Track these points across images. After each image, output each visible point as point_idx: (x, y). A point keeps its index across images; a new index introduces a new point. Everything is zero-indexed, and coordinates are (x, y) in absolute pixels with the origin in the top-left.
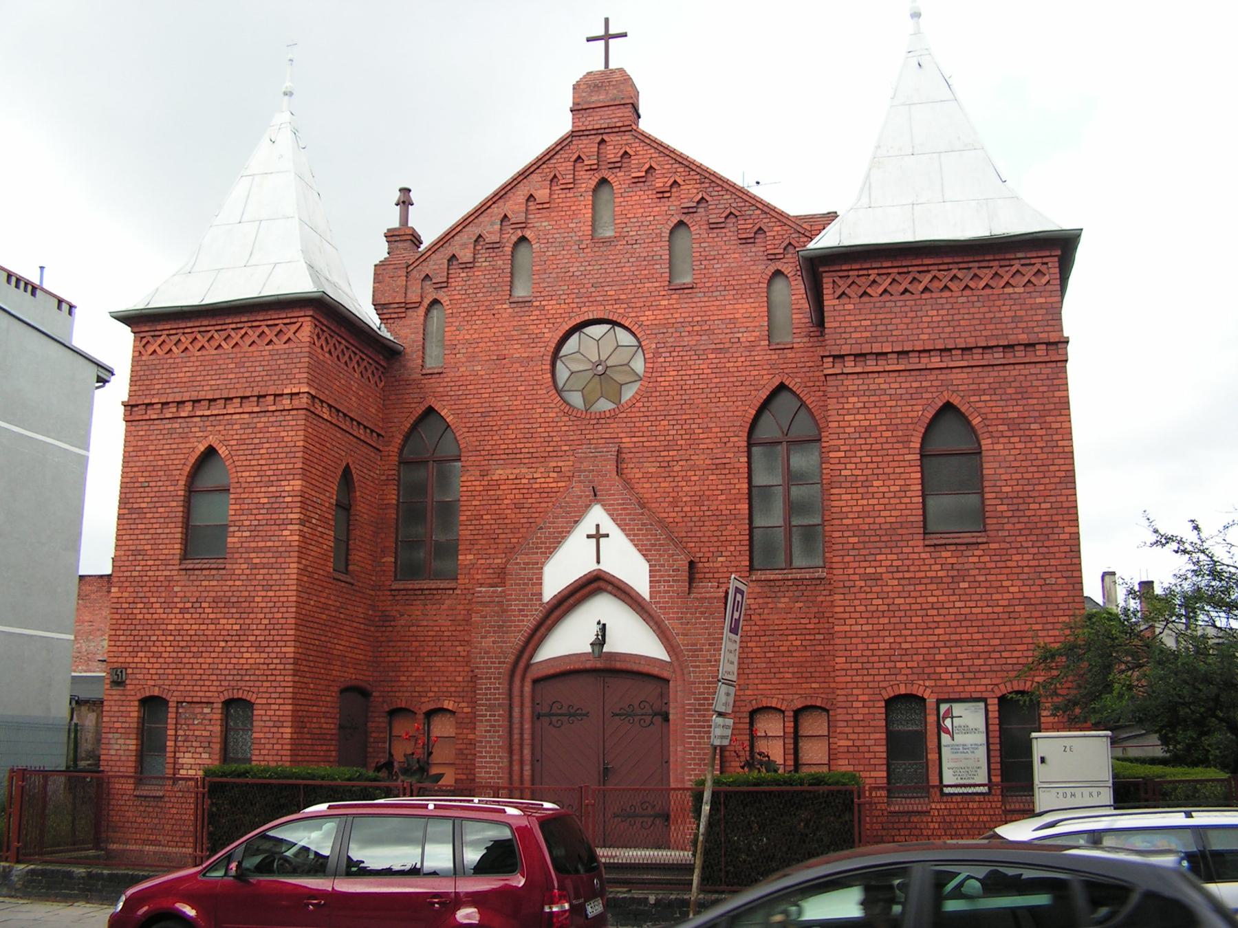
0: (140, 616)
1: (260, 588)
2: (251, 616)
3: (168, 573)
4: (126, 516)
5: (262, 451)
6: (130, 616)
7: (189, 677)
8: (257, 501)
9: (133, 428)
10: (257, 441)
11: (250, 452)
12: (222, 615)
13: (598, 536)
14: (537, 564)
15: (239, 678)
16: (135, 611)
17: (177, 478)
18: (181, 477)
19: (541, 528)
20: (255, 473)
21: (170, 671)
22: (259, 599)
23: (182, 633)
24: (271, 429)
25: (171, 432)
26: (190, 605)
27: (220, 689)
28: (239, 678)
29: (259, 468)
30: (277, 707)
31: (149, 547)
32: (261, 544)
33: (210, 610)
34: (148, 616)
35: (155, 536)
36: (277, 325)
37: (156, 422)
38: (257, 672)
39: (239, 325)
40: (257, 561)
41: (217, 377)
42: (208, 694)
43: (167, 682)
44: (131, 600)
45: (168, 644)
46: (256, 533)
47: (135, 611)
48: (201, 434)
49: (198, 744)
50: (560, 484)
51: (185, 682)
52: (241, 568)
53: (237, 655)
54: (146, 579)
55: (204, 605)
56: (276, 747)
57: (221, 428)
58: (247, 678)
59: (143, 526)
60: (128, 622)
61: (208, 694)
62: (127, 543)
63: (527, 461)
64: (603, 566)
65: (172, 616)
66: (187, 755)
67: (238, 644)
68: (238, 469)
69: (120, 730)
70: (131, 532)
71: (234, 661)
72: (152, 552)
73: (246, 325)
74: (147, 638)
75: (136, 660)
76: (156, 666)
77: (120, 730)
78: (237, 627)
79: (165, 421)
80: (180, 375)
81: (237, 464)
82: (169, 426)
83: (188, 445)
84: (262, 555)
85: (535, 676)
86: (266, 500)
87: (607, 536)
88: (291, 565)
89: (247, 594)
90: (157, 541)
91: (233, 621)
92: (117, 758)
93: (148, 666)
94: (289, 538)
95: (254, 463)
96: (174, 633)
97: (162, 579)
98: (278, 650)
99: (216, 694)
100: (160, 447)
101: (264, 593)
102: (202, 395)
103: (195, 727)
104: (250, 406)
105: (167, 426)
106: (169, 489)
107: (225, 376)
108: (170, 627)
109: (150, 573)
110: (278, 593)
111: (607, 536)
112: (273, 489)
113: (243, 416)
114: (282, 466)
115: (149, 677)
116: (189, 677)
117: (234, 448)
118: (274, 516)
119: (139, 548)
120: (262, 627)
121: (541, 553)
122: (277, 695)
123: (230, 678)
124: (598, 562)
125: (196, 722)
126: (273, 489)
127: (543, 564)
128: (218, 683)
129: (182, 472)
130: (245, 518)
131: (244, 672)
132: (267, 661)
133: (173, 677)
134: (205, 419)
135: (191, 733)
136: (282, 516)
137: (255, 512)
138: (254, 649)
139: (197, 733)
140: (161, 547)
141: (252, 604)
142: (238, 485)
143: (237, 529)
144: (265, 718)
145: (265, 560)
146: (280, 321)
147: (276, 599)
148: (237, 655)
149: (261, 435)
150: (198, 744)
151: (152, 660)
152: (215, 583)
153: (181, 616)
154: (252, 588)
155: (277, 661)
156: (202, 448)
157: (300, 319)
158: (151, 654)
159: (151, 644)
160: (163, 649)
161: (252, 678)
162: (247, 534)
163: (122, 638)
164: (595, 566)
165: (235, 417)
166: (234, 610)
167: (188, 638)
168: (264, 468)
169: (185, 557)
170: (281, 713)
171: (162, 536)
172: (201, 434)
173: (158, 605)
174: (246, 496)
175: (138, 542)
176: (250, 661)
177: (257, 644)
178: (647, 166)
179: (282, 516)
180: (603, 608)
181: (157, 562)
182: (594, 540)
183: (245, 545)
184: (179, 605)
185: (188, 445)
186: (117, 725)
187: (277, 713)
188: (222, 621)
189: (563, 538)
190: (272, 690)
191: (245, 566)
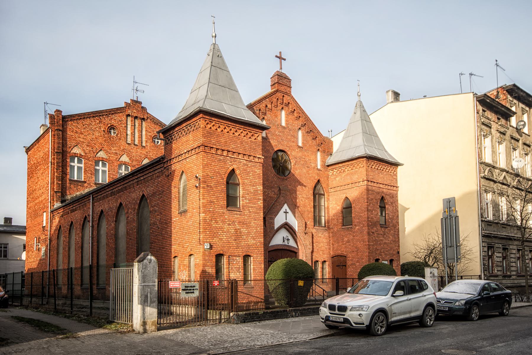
0: (214, 225)
1: (253, 219)
2: (250, 228)
3: (223, 211)
4: (206, 188)
5: (251, 174)
6: (210, 225)
7: (232, 247)
8: (250, 191)
9: (205, 155)
10: (248, 170)
11: (246, 174)
12: (242, 227)
13: (286, 212)
14: (273, 218)
15: (248, 248)
16: (212, 223)
17: (223, 177)
18: (225, 177)
19: (274, 208)
20: (249, 181)
21: (226, 245)
22: (253, 223)
23: (229, 232)
24: (252, 168)
25: (220, 160)
26: (231, 223)
27: (242, 252)
28: (248, 248)
29: (250, 180)
30: (259, 258)
31: (215, 201)
32: (252, 205)
33: (238, 225)
34: (217, 225)
35: (217, 197)
36: (252, 132)
37: (214, 155)
38: (253, 247)
39: (240, 128)
40: (251, 210)
41: (234, 144)
42: (239, 253)
43: (225, 249)
44: (210, 219)
45: (224, 236)
46: (250, 201)
47: (212, 223)
48: (230, 163)
49: (236, 270)
50: (275, 196)
51: (231, 249)
52: (247, 212)
53: (247, 241)
54: (214, 212)
55: (236, 223)
56: (260, 270)
57: (237, 163)
58: (251, 248)
59: (212, 193)
60: (210, 227)
61: (239, 253)
62: (207, 198)
63: (267, 187)
64: (287, 221)
65: (225, 226)
66: (232, 274)
67: (247, 237)
68: (244, 179)
69: (209, 266)
70: (208, 194)
71: (246, 243)
72: (217, 203)
73: (242, 129)
74: (217, 233)
75: (213, 241)
76: (221, 243)
77: (209, 266)
78: (247, 232)
79: (217, 155)
80: (221, 140)
81: (244, 177)
82: (219, 158)
83: (226, 166)
84: (252, 209)
85: (269, 250)
86: (253, 191)
87: (288, 213)
88: (261, 213)
89: (249, 221)
90: (218, 199)
91: (245, 229)
92: (209, 276)
93: (218, 243)
94: (260, 205)
95: (248, 178)
96: (226, 232)
97: (221, 212)
98: (259, 240)
99: (241, 253)
100: (216, 165)
101: (254, 221)
102: (230, 149)
103: (235, 264)
104: (246, 158)
105: (218, 157)
106: (221, 181)
107: (237, 145)
108: (225, 230)
109: (216, 210)
110: (258, 222)
111: (288, 213)
112: (255, 188)
113: (243, 161)
114: (257, 181)
115: (219, 247)
116: (232, 247)
117: (242, 171)
118: (256, 197)
119: (212, 200)
120: (254, 232)
121: (274, 215)
122: (259, 254)
123: (245, 248)
124: (286, 220)
125: (234, 263)
126: (255, 188)
127: (275, 218)
128: (242, 250)
129: (225, 176)
130: (247, 196)
131: (249, 246)
132: (256, 243)
133: (227, 247)
134: (232, 158)
135: (233, 266)
136: (258, 197)
137: (250, 194)
138: (252, 239)
139: (235, 266)
140: (220, 201)
141: (251, 225)
142: (244, 184)
143: (244, 199)
144: (256, 261)
145: (253, 211)
146: (253, 131)
147: (258, 224)
148: (247, 241)
149: (250, 169)
150: (236, 270)
151: (219, 241)
152: (238, 216)
153: (228, 226)
154: (250, 219)
155: (258, 243)
156: (231, 168)
157: (259, 133)
158: (219, 239)
159: (219, 235)
160: (223, 237)
161: (252, 248)
162: (248, 201)
163: (208, 233)
164: (285, 221)
165: (241, 160)
166: (245, 226)
167: (231, 234)
168: (251, 180)
169: (227, 207)
170: (261, 260)
171: (220, 197)
172: (229, 163)
173: (220, 222)
174: (247, 188)
175: (211, 198)
176: (251, 243)
177: (253, 237)
178: (294, 109)
179: (258, 197)
180: (284, 233)
181: (218, 206)
182: (285, 213)
183: (248, 205)
184: (227, 222)
185: (226, 166)
186: (208, 264)
187: (260, 260)
188: (242, 229)
189: (279, 212)
190: (258, 252)
191: (247, 212)
